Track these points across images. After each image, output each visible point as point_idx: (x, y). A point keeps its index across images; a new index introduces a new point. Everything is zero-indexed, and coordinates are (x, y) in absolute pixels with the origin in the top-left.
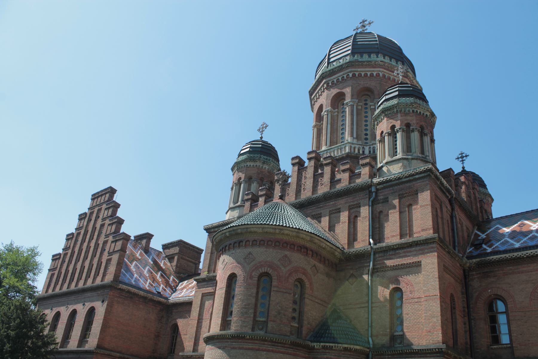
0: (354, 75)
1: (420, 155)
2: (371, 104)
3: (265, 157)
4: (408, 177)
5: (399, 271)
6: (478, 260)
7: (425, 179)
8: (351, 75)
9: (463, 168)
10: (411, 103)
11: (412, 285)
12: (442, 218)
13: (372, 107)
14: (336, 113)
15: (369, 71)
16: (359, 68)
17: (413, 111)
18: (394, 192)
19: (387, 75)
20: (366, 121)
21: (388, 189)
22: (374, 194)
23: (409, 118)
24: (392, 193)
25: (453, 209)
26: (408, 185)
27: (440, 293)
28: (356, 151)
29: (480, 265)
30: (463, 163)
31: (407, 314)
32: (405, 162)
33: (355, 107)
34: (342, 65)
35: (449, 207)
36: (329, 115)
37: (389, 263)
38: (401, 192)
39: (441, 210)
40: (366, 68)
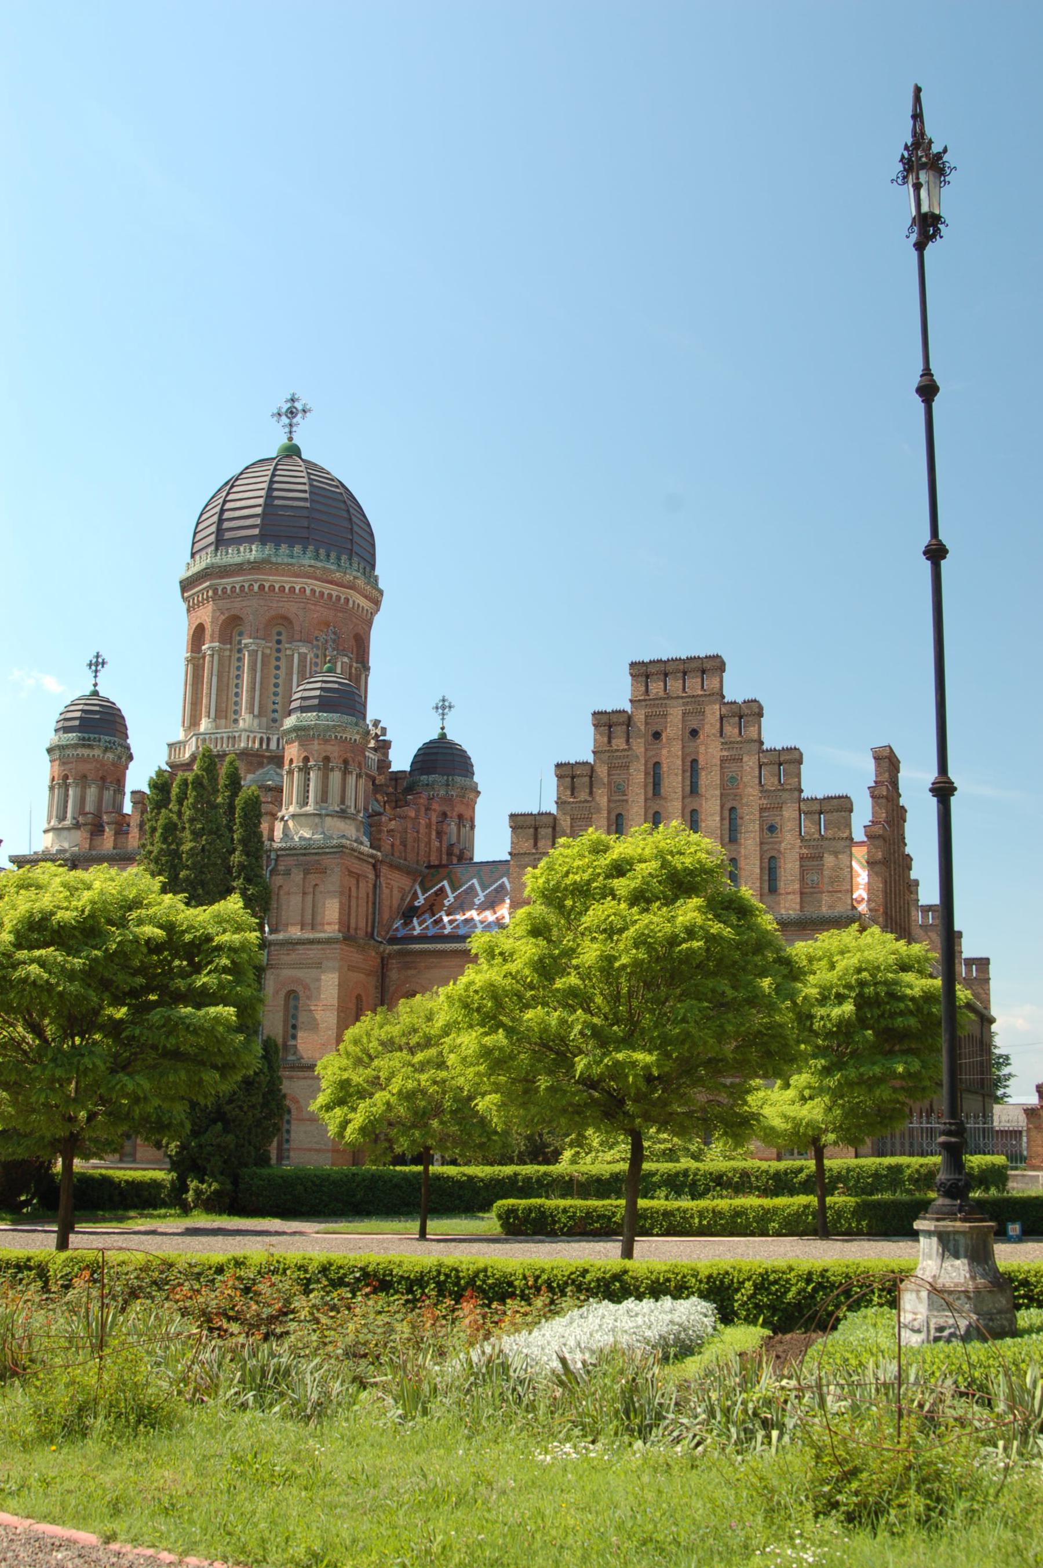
0: (262, 587)
1: (338, 809)
2: (287, 646)
3: (107, 738)
6: (399, 947)
7: (337, 856)
8: (256, 588)
9: (443, 728)
10: (334, 726)
12: (357, 898)
13: (288, 652)
14: (227, 653)
15: (287, 582)
16: (270, 575)
17: (336, 737)
19: (318, 590)
20: (277, 677)
22: (273, 862)
23: (329, 748)
25: (377, 876)
26: (317, 858)
27: (339, 1002)
28: (257, 745)
29: (401, 953)
30: (443, 719)
32: (317, 820)
33: (260, 653)
35: (371, 876)
36: (216, 657)
37: (285, 959)
39: (358, 888)
40: (283, 576)
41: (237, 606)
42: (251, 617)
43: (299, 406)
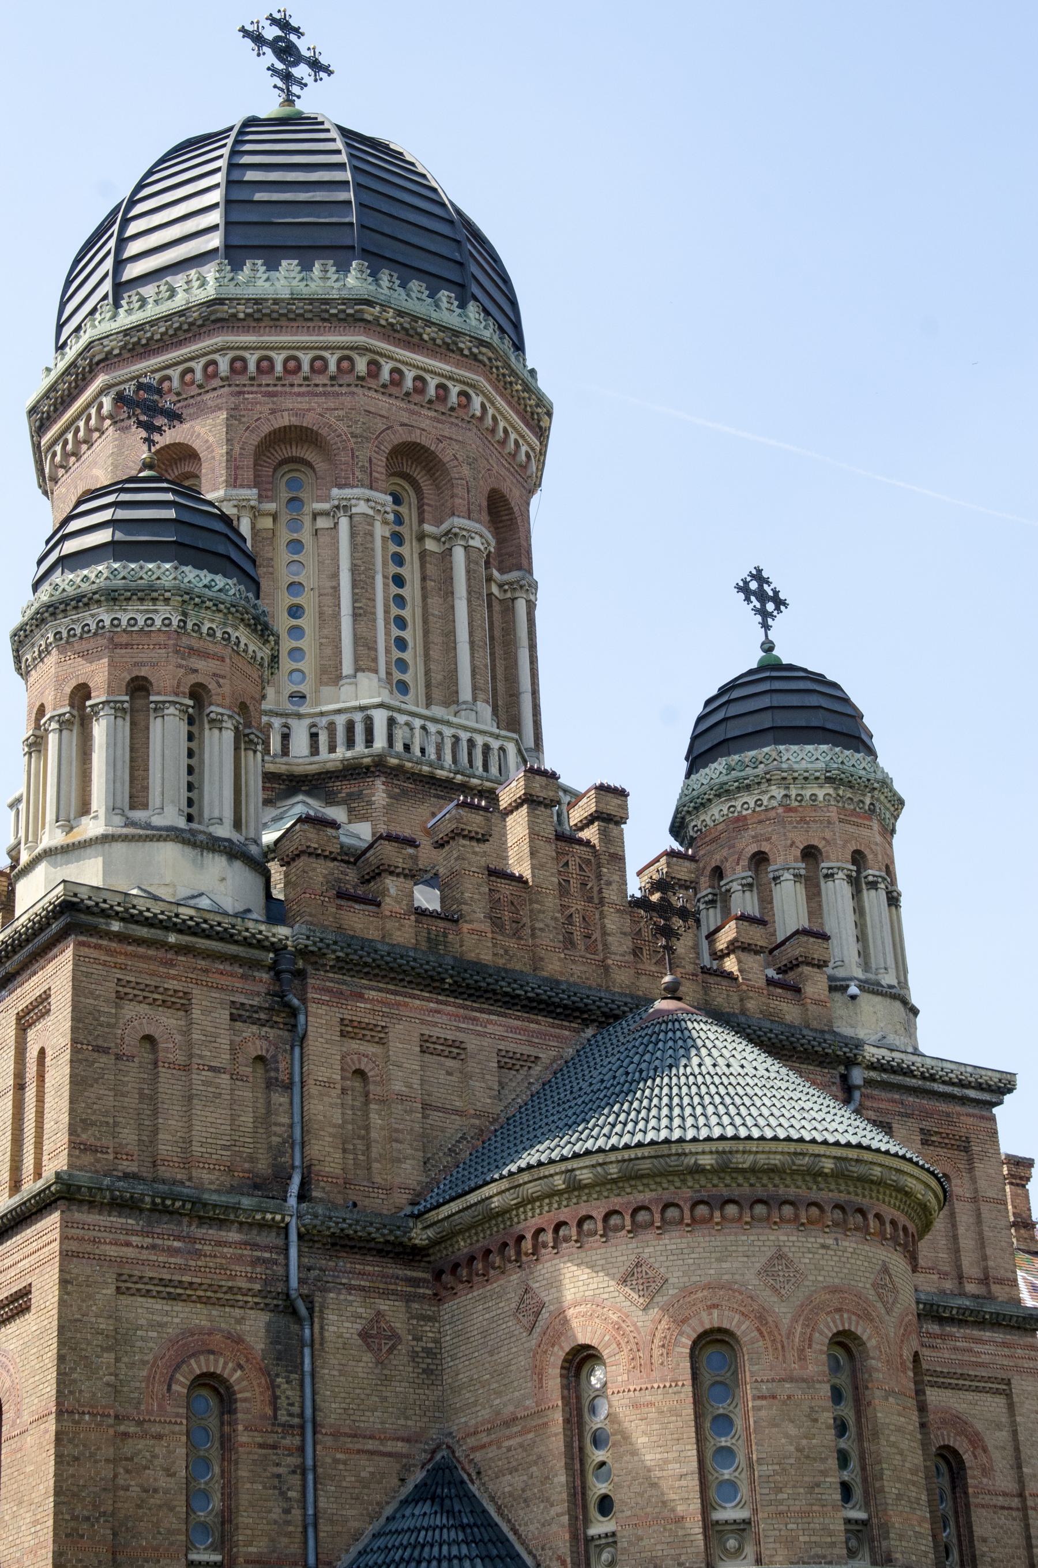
4: (953, 1084)
5: (949, 1393)
11: (985, 1450)
18: (908, 1116)
21: (889, 1095)
24: (901, 1114)
26: (943, 1107)
31: (984, 1540)
34: (456, 333)
38: (924, 1124)
41: (426, 428)
42: (466, 471)
43: (302, 45)
